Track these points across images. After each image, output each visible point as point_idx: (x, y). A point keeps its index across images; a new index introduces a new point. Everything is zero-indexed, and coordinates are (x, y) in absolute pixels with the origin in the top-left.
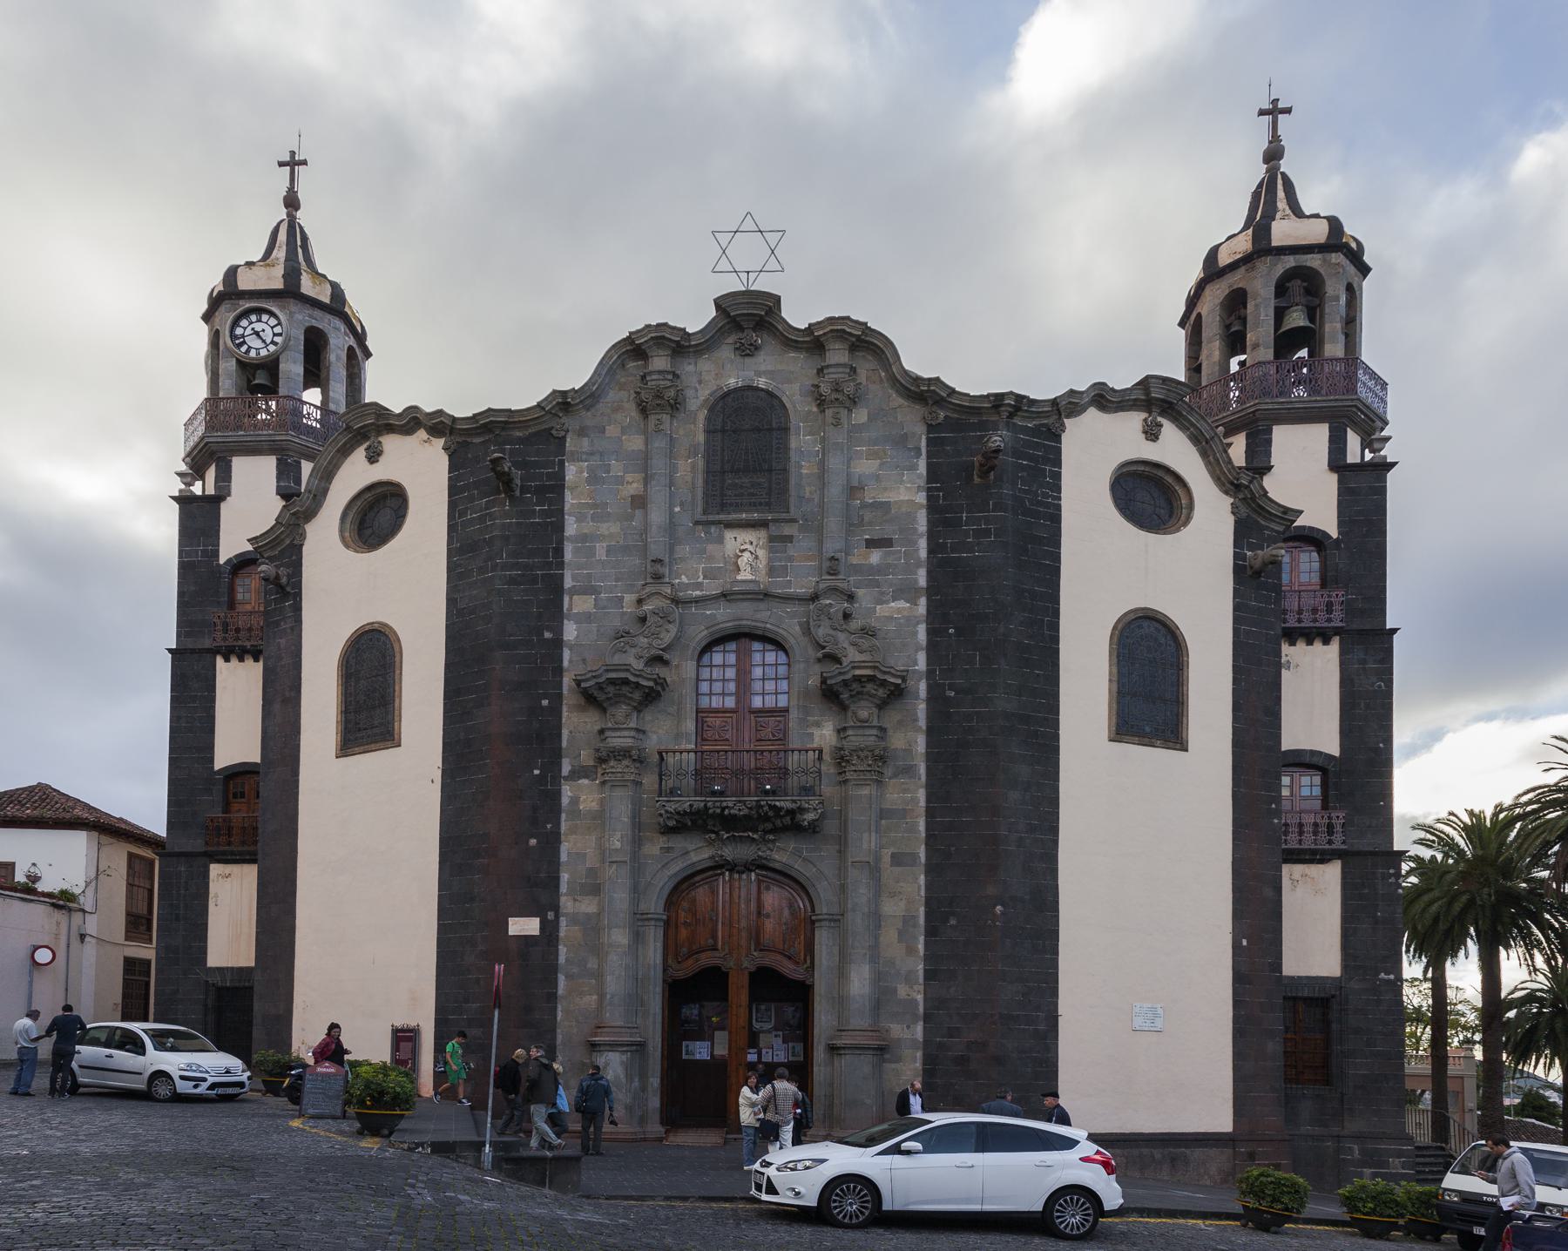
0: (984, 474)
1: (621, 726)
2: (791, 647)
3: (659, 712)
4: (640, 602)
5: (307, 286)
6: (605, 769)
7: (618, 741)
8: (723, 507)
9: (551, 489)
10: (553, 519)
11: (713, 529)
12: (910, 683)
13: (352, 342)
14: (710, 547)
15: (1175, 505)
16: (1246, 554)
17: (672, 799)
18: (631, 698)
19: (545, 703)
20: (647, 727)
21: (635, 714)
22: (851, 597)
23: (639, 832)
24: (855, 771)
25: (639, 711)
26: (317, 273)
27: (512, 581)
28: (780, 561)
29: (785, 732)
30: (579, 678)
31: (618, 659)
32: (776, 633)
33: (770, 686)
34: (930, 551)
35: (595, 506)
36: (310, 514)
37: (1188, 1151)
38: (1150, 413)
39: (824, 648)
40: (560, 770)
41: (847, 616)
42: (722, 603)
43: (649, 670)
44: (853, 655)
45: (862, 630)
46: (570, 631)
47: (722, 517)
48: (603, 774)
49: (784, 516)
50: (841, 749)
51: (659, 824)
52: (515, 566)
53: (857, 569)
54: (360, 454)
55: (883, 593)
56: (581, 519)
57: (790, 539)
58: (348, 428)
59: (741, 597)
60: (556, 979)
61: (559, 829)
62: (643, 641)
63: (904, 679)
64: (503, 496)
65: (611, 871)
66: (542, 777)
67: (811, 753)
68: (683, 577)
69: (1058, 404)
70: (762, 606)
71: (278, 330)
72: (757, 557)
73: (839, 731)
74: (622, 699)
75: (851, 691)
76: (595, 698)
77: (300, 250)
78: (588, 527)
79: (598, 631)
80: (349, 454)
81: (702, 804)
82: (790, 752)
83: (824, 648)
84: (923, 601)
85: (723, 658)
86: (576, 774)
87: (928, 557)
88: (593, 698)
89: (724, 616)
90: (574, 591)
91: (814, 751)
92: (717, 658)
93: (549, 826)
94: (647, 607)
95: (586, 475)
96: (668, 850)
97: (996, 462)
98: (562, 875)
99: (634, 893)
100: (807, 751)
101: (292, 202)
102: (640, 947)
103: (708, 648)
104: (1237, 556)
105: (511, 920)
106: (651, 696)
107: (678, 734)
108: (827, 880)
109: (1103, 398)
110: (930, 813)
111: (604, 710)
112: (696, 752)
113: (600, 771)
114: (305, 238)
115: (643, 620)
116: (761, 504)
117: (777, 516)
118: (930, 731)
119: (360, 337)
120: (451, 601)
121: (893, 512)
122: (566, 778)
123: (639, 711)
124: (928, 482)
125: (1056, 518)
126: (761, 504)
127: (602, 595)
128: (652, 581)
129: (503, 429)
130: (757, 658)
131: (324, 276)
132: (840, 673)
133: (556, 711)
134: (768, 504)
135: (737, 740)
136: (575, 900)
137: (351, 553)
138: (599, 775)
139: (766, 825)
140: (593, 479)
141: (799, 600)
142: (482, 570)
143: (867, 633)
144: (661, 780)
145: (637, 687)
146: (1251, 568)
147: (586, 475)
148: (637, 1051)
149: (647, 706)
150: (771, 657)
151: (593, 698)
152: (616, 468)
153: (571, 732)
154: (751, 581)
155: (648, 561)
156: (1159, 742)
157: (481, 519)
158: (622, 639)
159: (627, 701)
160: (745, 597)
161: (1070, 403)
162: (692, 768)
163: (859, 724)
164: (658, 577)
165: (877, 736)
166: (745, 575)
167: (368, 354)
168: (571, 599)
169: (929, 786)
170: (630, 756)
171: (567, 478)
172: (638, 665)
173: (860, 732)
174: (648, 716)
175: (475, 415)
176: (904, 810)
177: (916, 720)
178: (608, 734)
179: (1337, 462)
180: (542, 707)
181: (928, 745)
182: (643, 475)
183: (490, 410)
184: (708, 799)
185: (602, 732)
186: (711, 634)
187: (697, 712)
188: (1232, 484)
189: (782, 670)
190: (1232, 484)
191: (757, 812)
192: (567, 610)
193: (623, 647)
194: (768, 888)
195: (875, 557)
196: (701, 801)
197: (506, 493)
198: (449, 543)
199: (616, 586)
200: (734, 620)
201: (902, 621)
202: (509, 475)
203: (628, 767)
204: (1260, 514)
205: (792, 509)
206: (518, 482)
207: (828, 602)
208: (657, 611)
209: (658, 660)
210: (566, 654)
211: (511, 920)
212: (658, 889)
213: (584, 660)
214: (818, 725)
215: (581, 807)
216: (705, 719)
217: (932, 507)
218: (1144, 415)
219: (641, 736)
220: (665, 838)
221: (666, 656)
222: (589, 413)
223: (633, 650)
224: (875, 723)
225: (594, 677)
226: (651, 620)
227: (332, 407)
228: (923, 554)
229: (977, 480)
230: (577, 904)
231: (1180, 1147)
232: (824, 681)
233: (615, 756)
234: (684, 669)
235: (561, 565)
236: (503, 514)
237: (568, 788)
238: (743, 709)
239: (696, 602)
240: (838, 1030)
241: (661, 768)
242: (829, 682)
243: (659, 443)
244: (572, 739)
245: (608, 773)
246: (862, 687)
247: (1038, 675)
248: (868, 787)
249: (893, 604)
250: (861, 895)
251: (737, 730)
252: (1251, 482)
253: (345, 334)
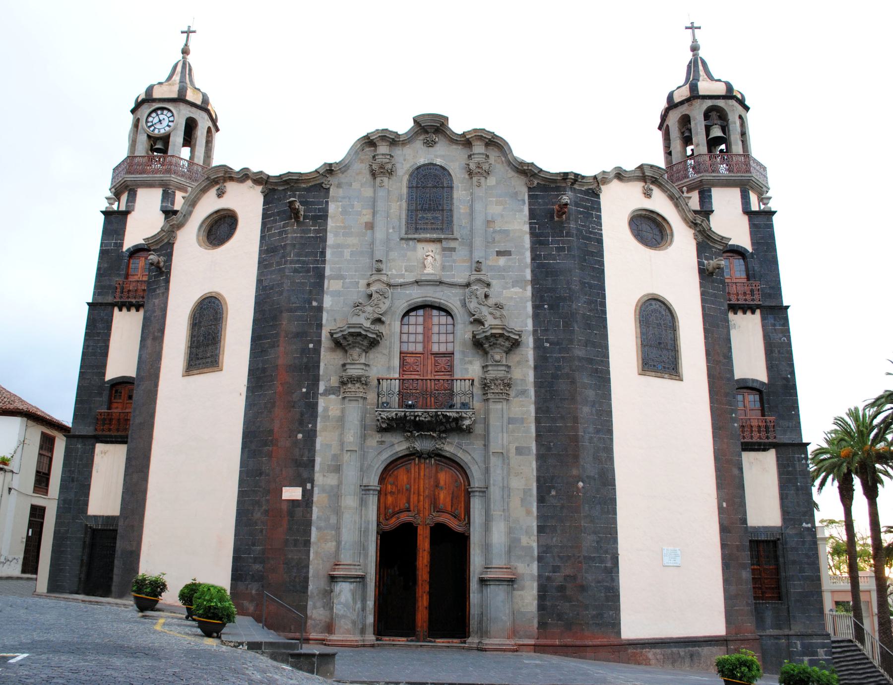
0: (560, 216)
1: (356, 362)
2: (455, 314)
3: (378, 353)
4: (369, 285)
5: (190, 96)
7: (353, 371)
8: (416, 230)
9: (320, 217)
11: (411, 243)
12: (524, 338)
13: (210, 124)
14: (409, 253)
15: (664, 233)
16: (704, 262)
17: (385, 410)
18: (362, 345)
19: (311, 346)
20: (371, 363)
21: (364, 354)
22: (488, 285)
23: (365, 430)
24: (493, 393)
25: (366, 352)
26: (195, 88)
27: (296, 271)
28: (449, 262)
29: (452, 367)
30: (332, 331)
31: (355, 320)
32: (447, 306)
33: (443, 338)
34: (533, 259)
35: (345, 228)
36: (180, 226)
37: (700, 649)
38: (646, 182)
39: (474, 315)
40: (318, 389)
41: (486, 296)
42: (416, 287)
43: (373, 327)
44: (490, 321)
45: (495, 305)
46: (328, 302)
47: (416, 236)
48: (344, 392)
49: (450, 236)
50: (485, 379)
51: (377, 426)
52: (298, 262)
53: (492, 268)
54: (213, 192)
55: (507, 283)
56: (336, 235)
57: (453, 250)
58: (208, 178)
59: (426, 283)
61: (316, 428)
62: (369, 309)
63: (520, 336)
64: (293, 220)
65: (346, 457)
66: (307, 393)
67: (467, 381)
68: (393, 270)
69: (597, 179)
70: (439, 289)
71: (171, 119)
72: (435, 260)
73: (483, 367)
74: (357, 345)
75: (490, 342)
76: (341, 344)
77: (187, 76)
79: (344, 302)
80: (207, 192)
81: (403, 414)
82: (455, 381)
83: (474, 315)
84: (529, 288)
85: (417, 318)
86: (329, 391)
87: (531, 263)
88: (340, 344)
89: (418, 295)
90: (332, 278)
91: (469, 380)
92: (412, 320)
93: (310, 426)
94: (373, 288)
95: (340, 210)
96: (382, 443)
97: (566, 210)
99: (361, 471)
100: (465, 380)
101: (185, 51)
102: (363, 508)
103: (407, 314)
104: (700, 263)
105: (284, 489)
106: (373, 343)
107: (389, 367)
108: (477, 464)
109: (620, 175)
110: (538, 420)
111: (346, 351)
112: (400, 380)
113: (342, 390)
114: (190, 70)
115: (370, 296)
116: (437, 229)
117: (446, 236)
118: (536, 368)
119: (214, 121)
120: (259, 281)
121: (511, 235)
122: (321, 395)
123: (366, 352)
124: (530, 219)
125: (600, 242)
126: (437, 229)
127: (347, 280)
128: (376, 273)
130: (435, 320)
131: (199, 90)
132: (484, 332)
133: (317, 351)
134: (442, 229)
135: (423, 372)
137: (202, 249)
138: (341, 393)
139: (441, 427)
140: (344, 212)
141: (460, 286)
142: (279, 264)
143: (498, 307)
144: (379, 397)
145: (366, 338)
146: (708, 270)
147: (340, 210)
148: (360, 582)
149: (371, 349)
150: (444, 319)
151: (340, 344)
152: (358, 206)
153: (325, 365)
154: (432, 274)
155: (374, 260)
156: (666, 375)
157: (280, 233)
158: (358, 308)
159: (360, 346)
160: (429, 283)
161: (603, 178)
162: (397, 390)
163: (495, 363)
164: (379, 271)
165: (505, 371)
166: (429, 270)
167: (217, 130)
168: (329, 282)
169: (536, 403)
170: (361, 381)
171: (329, 211)
172: (367, 324)
173: (495, 368)
174: (371, 355)
176: (522, 418)
177: (527, 361)
178: (348, 366)
179: (747, 211)
180: (309, 349)
181: (536, 377)
182: (372, 210)
184: (407, 410)
185: (344, 365)
186: (409, 305)
187: (400, 353)
188: (692, 222)
189: (450, 328)
190: (692, 222)
191: (436, 419)
192: (327, 289)
193: (358, 312)
194: (442, 470)
195: (502, 261)
196: (402, 411)
197: (295, 219)
198: (261, 246)
199: (355, 275)
200: (422, 297)
201: (518, 300)
202: (298, 209)
203: (359, 388)
204: (709, 240)
205: (455, 232)
206: (302, 213)
207: (476, 287)
208: (378, 291)
209: (378, 321)
210: (325, 316)
211: (284, 489)
212: (375, 470)
213: (335, 320)
214: (471, 362)
215: (330, 414)
216: (406, 358)
217: (533, 233)
218: (642, 184)
219: (367, 368)
220: (380, 435)
221: (383, 319)
222: (343, 175)
223: (364, 315)
224: (504, 363)
225: (341, 331)
226: (375, 296)
227: (196, 161)
228: (528, 260)
229: (556, 219)
231: (695, 646)
232: (474, 336)
233: (351, 381)
234: (393, 327)
235: (324, 262)
236: (293, 232)
237: (322, 400)
238: (428, 353)
239: (401, 286)
240: (485, 568)
241: (378, 389)
242: (477, 337)
243: (381, 193)
244: (326, 368)
245: (347, 392)
246: (496, 340)
247: (596, 334)
248: (501, 404)
249: (512, 290)
250: (497, 475)
251: (424, 365)
252: (702, 222)
253: (207, 120)
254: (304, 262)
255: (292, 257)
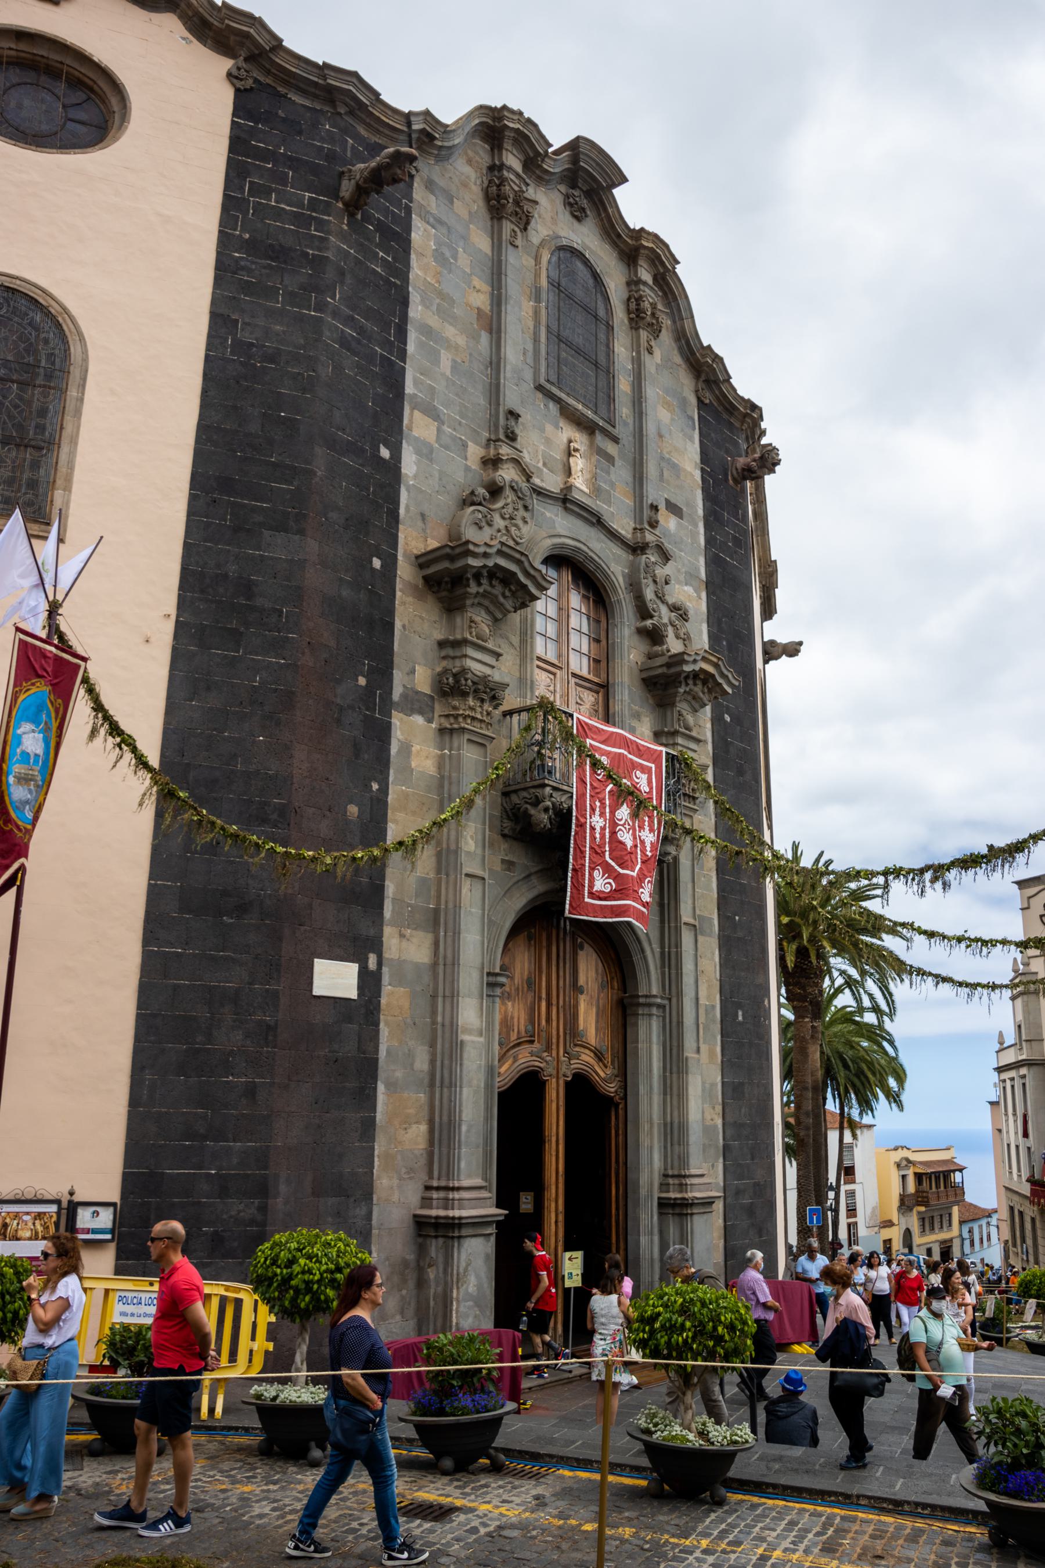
6: (455, 708)
10: (398, 282)
14: (549, 428)
27: (344, 342)
46: (409, 464)
52: (349, 321)
60: (375, 1089)
66: (369, 689)
78: (433, 321)
86: (414, 703)
98: (387, 883)
129: (351, 113)
136: (402, 936)
138: (436, 715)
175: (326, 65)
183: (355, 74)
215: (413, 765)
230: (404, 944)
254: (361, 331)
255: (335, 300)
